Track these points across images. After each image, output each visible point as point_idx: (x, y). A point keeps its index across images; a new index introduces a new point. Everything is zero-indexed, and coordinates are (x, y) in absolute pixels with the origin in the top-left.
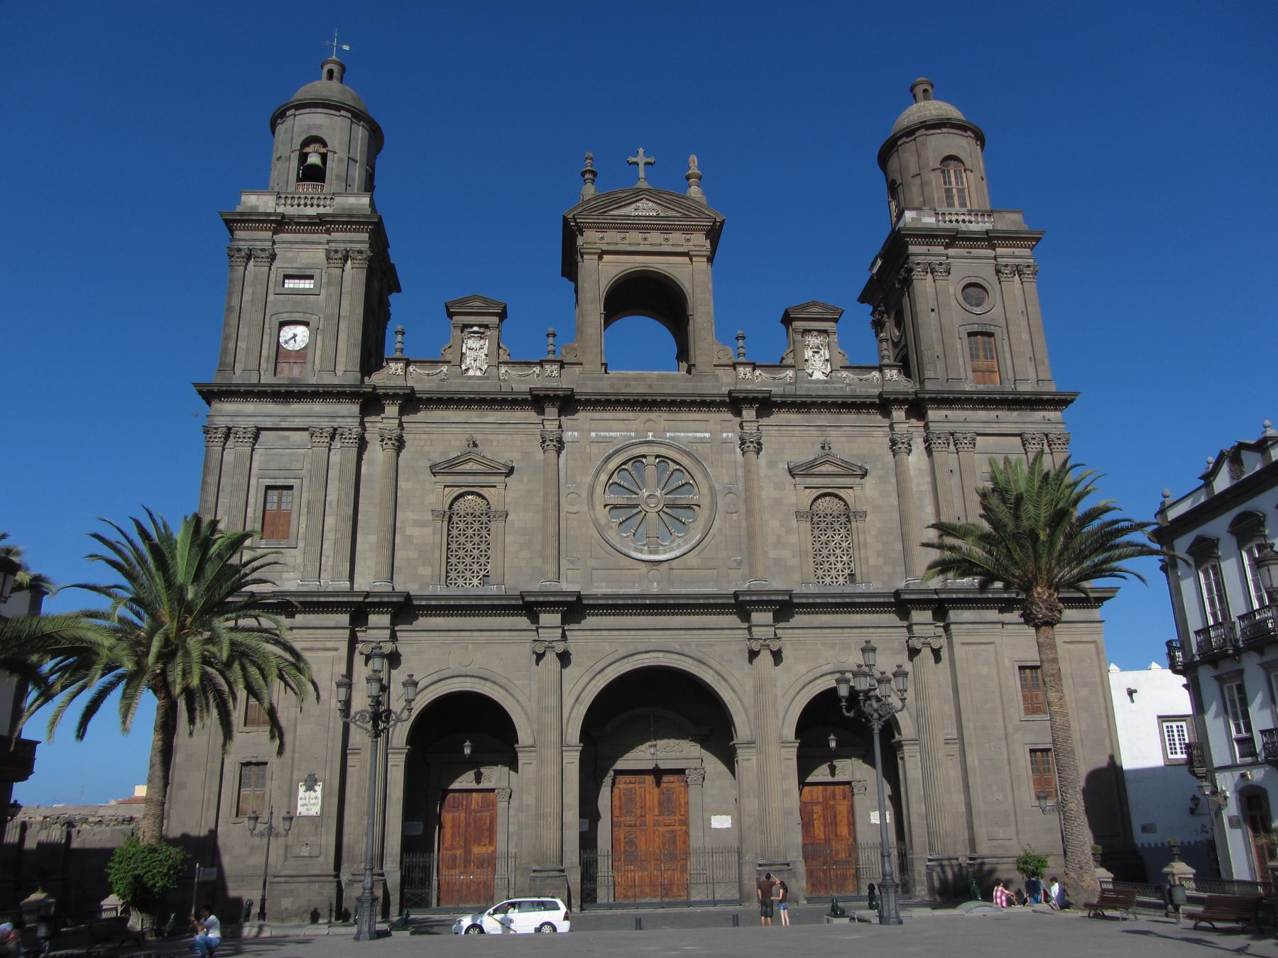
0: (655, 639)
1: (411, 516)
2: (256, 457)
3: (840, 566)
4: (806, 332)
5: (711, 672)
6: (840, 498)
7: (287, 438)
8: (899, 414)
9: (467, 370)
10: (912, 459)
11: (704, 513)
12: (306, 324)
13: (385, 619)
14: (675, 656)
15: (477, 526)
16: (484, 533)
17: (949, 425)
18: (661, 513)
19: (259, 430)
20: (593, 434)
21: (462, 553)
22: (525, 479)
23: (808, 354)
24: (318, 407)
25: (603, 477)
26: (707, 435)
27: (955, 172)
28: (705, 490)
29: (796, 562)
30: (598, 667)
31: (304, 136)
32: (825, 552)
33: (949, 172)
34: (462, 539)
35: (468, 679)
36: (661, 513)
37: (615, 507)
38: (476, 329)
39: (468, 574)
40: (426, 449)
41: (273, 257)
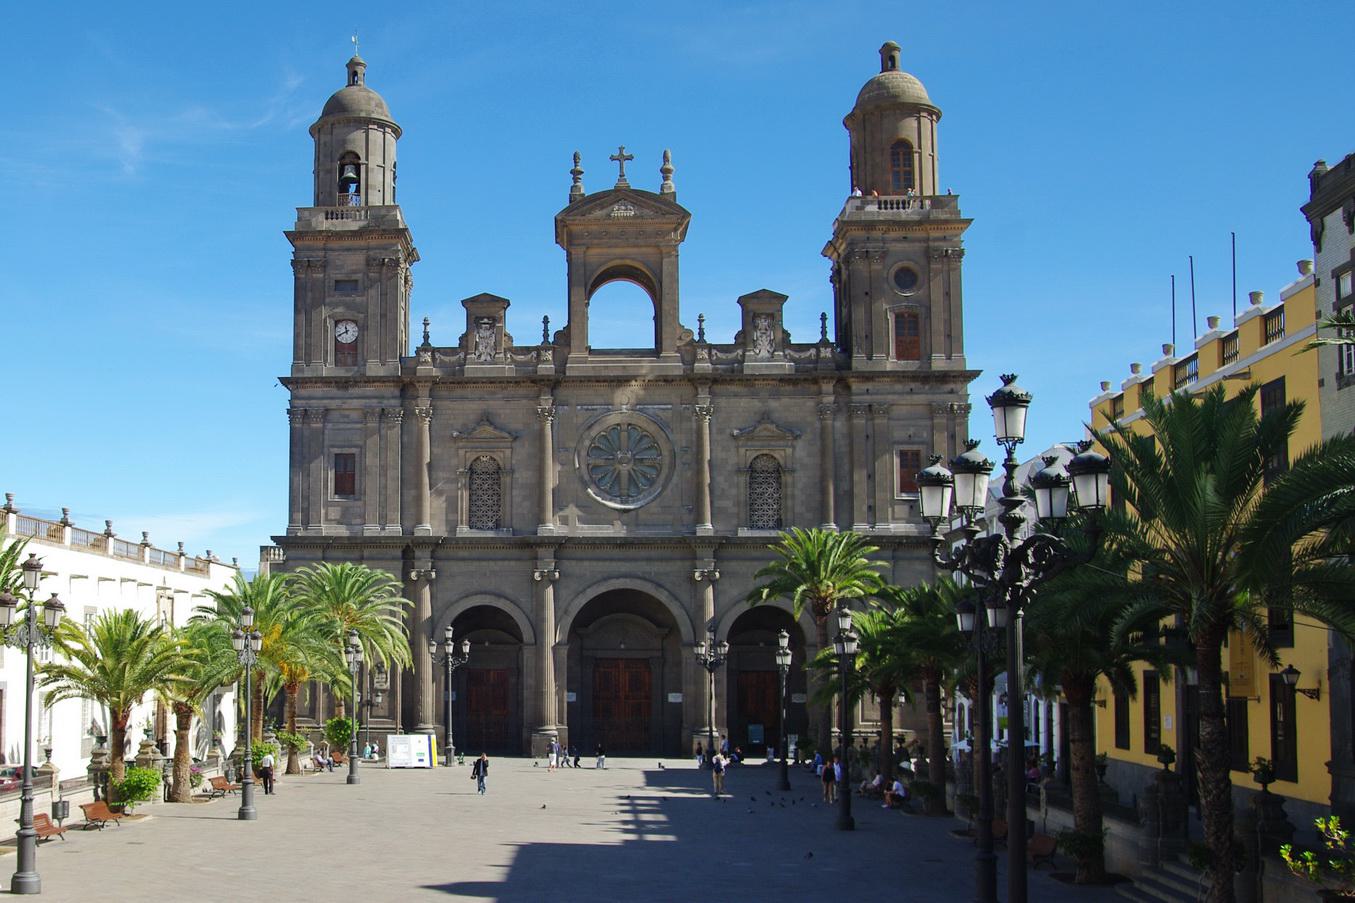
0: (625, 567)
1: (441, 474)
2: (326, 432)
3: (770, 512)
4: (756, 316)
5: (666, 593)
6: (772, 457)
7: (348, 416)
8: (828, 387)
9: (480, 356)
10: (838, 424)
11: (665, 471)
12: (355, 322)
13: (427, 553)
14: (639, 582)
15: (490, 482)
16: (496, 487)
17: (867, 398)
18: (632, 472)
19: (327, 410)
20: (579, 407)
21: (480, 503)
22: (527, 446)
23: (756, 334)
24: (370, 390)
25: (587, 443)
26: (669, 406)
27: (904, 154)
28: (665, 453)
29: (735, 510)
30: (581, 589)
31: (341, 152)
32: (760, 501)
33: (898, 154)
34: (480, 492)
35: (488, 597)
36: (632, 472)
37: (596, 467)
38: (486, 320)
39: (485, 518)
40: (451, 422)
41: (324, 266)
